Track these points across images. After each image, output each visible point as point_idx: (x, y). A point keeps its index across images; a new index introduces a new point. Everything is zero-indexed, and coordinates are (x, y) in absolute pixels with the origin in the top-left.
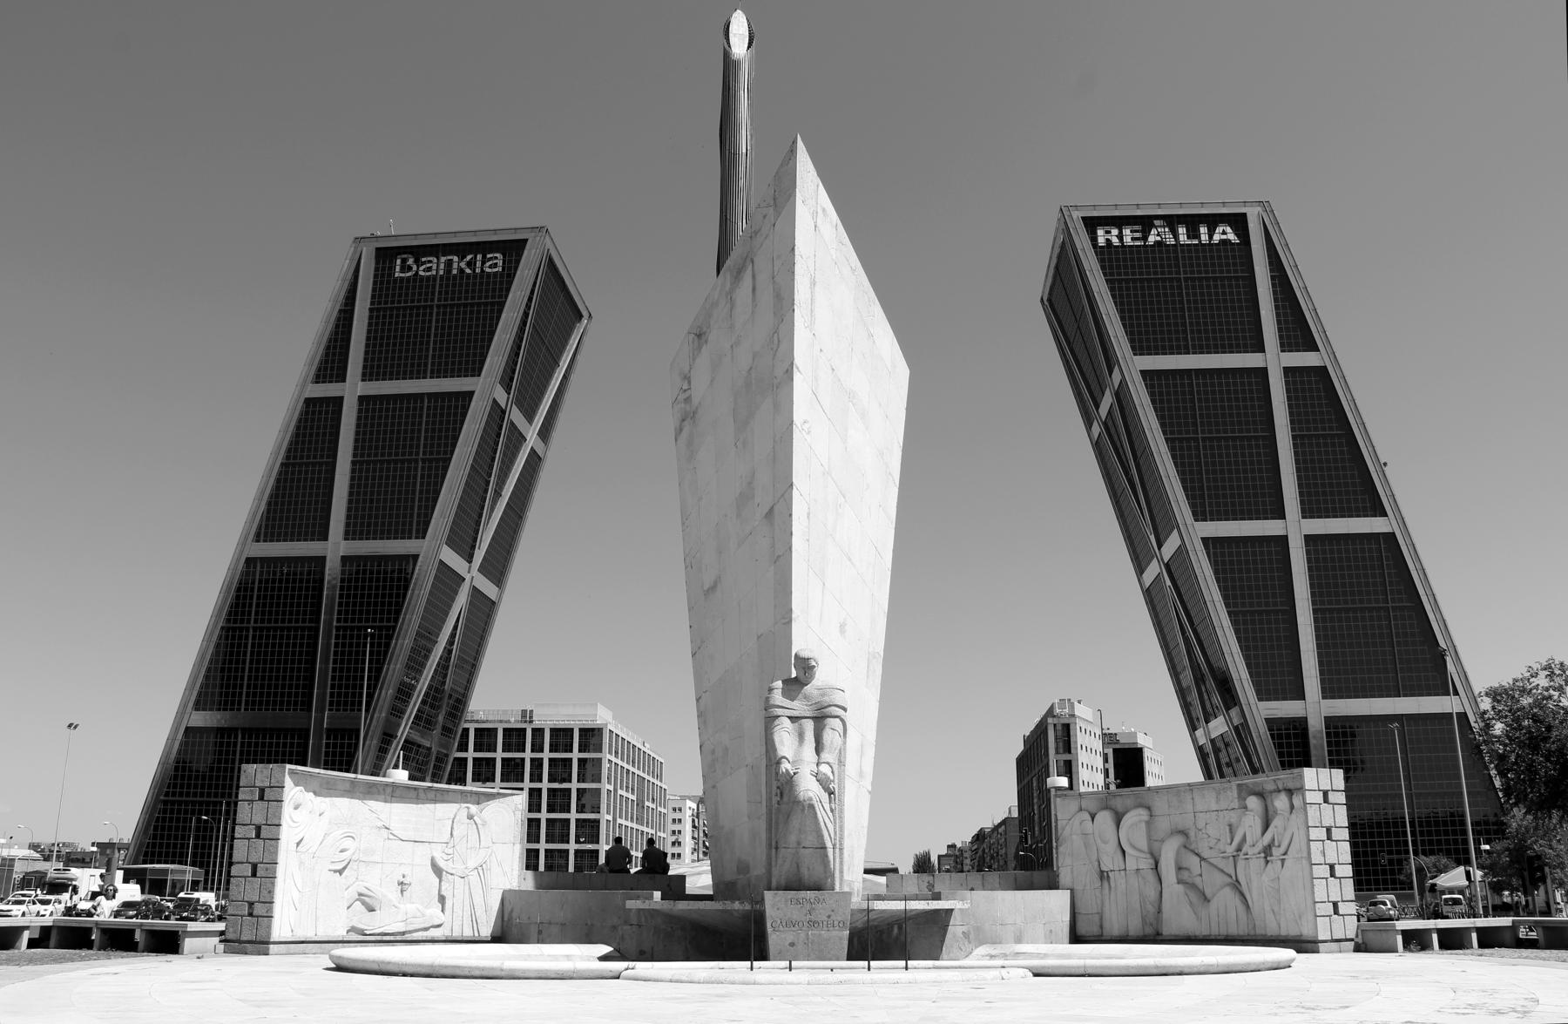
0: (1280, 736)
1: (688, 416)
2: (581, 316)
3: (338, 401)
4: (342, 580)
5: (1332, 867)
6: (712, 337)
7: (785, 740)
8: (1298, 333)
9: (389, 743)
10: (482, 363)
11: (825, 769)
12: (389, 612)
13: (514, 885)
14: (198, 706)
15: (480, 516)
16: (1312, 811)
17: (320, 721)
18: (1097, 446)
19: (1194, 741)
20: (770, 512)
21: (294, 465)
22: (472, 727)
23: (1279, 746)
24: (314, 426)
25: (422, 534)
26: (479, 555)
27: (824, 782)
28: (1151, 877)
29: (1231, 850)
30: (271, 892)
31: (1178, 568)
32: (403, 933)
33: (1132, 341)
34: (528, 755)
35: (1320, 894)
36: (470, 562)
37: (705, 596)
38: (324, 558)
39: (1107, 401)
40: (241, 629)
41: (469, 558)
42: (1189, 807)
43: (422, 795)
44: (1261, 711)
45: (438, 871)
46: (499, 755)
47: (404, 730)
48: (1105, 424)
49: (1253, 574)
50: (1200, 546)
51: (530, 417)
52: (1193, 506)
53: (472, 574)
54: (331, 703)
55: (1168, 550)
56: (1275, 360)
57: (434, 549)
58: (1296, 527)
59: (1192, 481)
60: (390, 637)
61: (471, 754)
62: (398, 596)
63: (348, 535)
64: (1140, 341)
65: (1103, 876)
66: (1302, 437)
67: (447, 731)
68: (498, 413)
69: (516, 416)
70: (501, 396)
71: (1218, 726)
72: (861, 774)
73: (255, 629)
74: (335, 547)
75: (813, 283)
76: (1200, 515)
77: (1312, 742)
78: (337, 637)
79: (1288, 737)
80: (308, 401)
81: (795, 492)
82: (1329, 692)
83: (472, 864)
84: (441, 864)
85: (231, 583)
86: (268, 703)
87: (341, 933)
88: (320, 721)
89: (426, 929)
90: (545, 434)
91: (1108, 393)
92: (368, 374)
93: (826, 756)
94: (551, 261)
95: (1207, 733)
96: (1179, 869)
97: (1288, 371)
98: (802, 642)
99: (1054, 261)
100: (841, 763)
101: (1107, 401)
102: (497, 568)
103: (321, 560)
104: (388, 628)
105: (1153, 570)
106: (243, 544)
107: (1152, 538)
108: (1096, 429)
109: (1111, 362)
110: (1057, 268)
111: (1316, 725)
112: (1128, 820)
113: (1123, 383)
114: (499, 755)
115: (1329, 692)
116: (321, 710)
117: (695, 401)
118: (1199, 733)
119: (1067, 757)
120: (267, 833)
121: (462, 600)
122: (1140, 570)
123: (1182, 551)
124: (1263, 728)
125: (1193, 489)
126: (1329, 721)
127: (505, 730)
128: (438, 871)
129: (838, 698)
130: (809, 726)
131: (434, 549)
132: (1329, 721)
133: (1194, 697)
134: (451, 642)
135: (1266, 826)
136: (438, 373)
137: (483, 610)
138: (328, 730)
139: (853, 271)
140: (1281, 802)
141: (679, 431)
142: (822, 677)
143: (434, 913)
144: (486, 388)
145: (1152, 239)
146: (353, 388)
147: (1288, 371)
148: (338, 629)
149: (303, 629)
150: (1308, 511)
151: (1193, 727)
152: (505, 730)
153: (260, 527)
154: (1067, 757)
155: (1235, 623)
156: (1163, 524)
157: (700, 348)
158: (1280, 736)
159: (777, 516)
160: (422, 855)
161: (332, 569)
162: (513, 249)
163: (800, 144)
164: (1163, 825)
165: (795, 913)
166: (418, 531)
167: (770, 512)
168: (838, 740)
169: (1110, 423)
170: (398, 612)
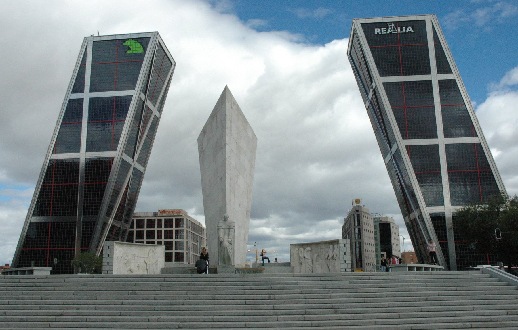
2: (172, 64)
3: (81, 101)
7: (221, 234)
8: (443, 67)
11: (230, 240)
14: (34, 215)
22: (135, 219)
26: (136, 156)
27: (230, 243)
30: (112, 268)
41: (133, 158)
44: (427, 211)
46: (146, 229)
47: (111, 221)
48: (371, 102)
55: (394, 149)
56: (435, 77)
58: (441, 141)
61: (135, 229)
62: (107, 172)
65: (301, 264)
69: (149, 104)
70: (143, 96)
72: (245, 239)
74: (83, 155)
76: (404, 137)
77: (447, 222)
80: (70, 100)
81: (227, 174)
83: (154, 262)
84: (147, 262)
91: (371, 90)
93: (231, 237)
94: (160, 44)
95: (409, 218)
100: (234, 238)
101: (371, 93)
104: (104, 184)
107: (388, 145)
108: (368, 104)
114: (146, 229)
119: (359, 227)
124: (428, 217)
129: (233, 224)
130: (227, 231)
135: (333, 252)
137: (139, 176)
145: (389, 32)
146: (87, 95)
169: (372, 102)
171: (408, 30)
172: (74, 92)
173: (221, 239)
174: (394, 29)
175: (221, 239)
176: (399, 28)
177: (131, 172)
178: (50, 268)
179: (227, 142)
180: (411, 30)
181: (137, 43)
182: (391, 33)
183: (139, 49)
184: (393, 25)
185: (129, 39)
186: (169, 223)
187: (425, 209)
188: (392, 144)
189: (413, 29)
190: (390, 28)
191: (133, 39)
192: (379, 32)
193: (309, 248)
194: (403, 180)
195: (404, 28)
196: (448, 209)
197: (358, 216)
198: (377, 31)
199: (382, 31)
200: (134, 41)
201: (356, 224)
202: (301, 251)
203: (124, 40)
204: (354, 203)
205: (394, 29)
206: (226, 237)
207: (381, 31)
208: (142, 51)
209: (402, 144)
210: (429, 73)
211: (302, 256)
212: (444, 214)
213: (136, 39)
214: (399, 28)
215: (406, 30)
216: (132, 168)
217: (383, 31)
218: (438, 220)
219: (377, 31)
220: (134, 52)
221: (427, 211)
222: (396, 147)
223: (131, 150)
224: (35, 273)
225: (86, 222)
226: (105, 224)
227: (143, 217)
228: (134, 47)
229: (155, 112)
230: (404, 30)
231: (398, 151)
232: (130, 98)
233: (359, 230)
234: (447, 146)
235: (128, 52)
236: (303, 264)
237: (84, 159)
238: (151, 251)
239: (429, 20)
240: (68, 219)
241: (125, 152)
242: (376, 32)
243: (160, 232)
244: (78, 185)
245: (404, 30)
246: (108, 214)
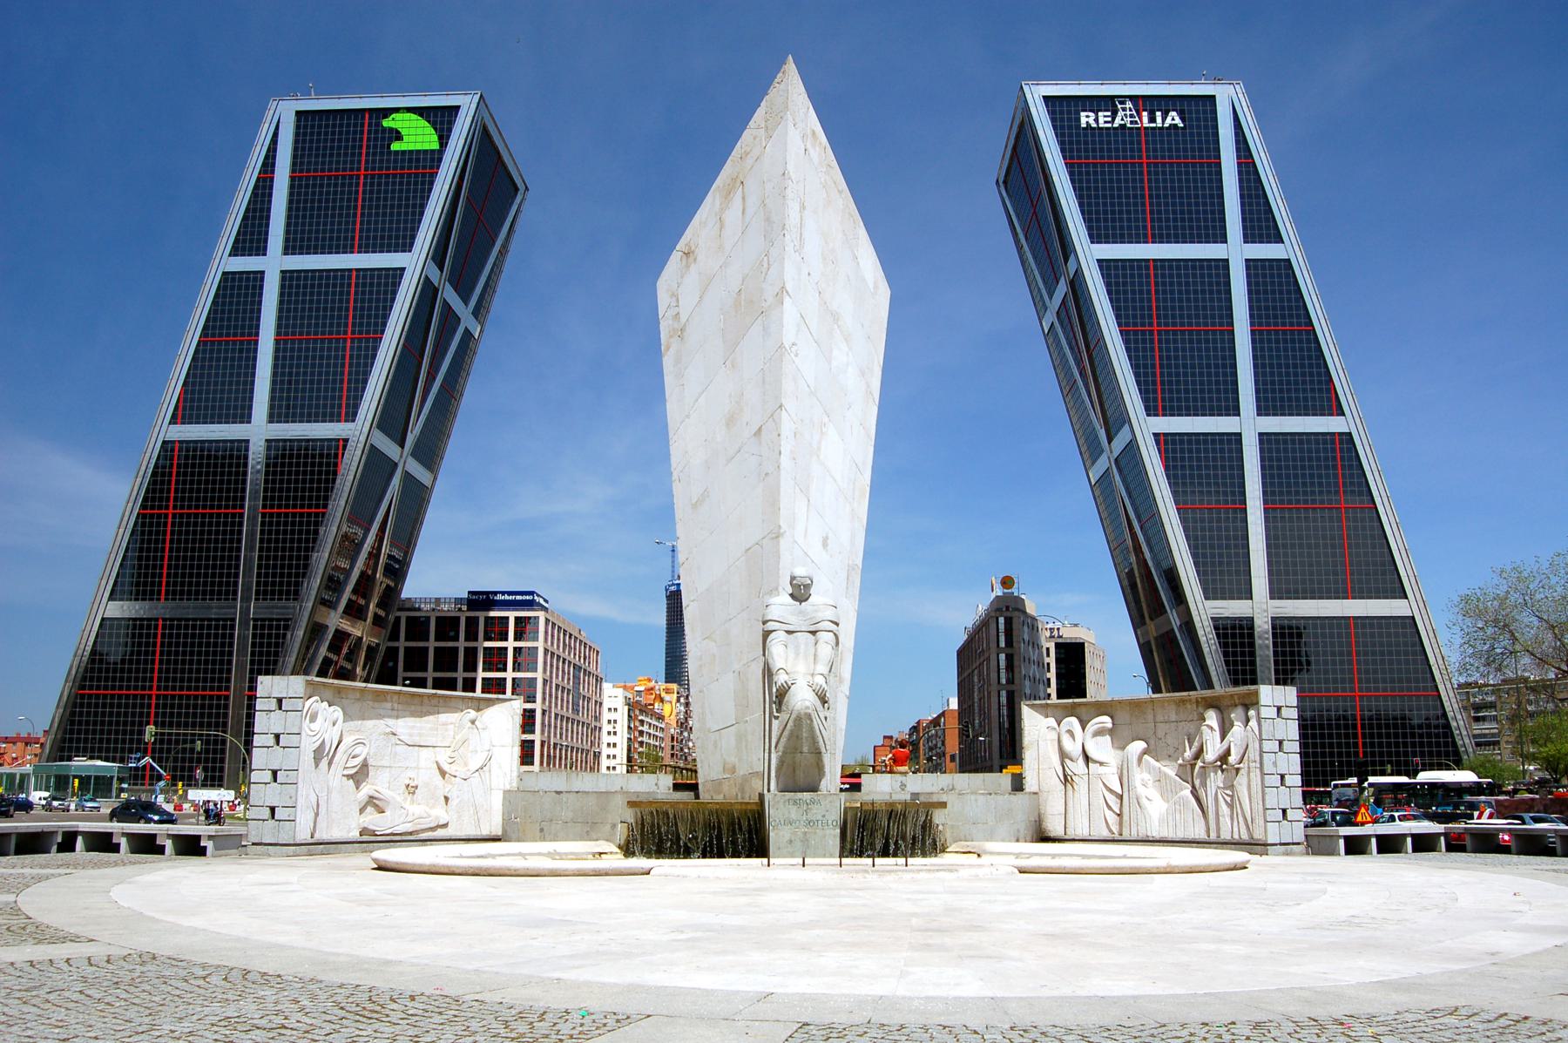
0: (1226, 636)
2: (517, 189)
4: (267, 465)
5: (1282, 777)
6: (701, 255)
8: (1260, 225)
10: (413, 237)
12: (318, 498)
16: (1265, 725)
23: (1224, 645)
25: (351, 416)
32: (411, 833)
33: (1089, 229)
34: (462, 644)
36: (402, 446)
41: (402, 446)
42: (1150, 717)
43: (426, 700)
46: (432, 644)
49: (1204, 468)
50: (1151, 441)
52: (1146, 401)
54: (258, 593)
56: (1236, 251)
58: (1249, 424)
59: (1146, 375)
63: (272, 418)
64: (1099, 228)
65: (1067, 780)
66: (1261, 332)
68: (428, 292)
69: (449, 294)
70: (435, 275)
74: (259, 431)
76: (1151, 410)
77: (1258, 642)
78: (263, 524)
82: (1276, 593)
84: (446, 767)
87: (354, 835)
89: (432, 829)
90: (476, 313)
92: (289, 249)
94: (485, 130)
97: (1250, 264)
101: (1062, 288)
102: (429, 453)
104: (317, 515)
105: (1103, 463)
108: (1050, 318)
109: (1067, 249)
111: (1262, 625)
113: (1079, 272)
114: (432, 644)
115: (1276, 593)
116: (246, 599)
117: (683, 319)
119: (1009, 651)
125: (1146, 383)
127: (438, 618)
137: (416, 499)
139: (840, 192)
143: (440, 814)
146: (274, 263)
148: (264, 516)
150: (1263, 409)
152: (438, 618)
154: (1009, 651)
156: (1115, 420)
157: (688, 266)
158: (1226, 636)
161: (257, 454)
165: (794, 813)
166: (347, 414)
170: (326, 498)
171: (1169, 121)
173: (781, 678)
175: (781, 678)
176: (1145, 114)
177: (396, 481)
180: (1178, 121)
181: (423, 123)
182: (1123, 127)
184: (1129, 105)
185: (397, 110)
188: (1113, 431)
189: (1183, 119)
190: (1121, 113)
192: (1091, 121)
193: (1106, 721)
195: (1158, 114)
198: (1086, 118)
199: (1101, 120)
200: (414, 116)
201: (1002, 644)
202: (1071, 733)
207: (1096, 120)
208: (436, 146)
209: (1146, 427)
210: (1223, 239)
211: (1073, 748)
214: (1145, 114)
215: (1164, 120)
218: (1236, 635)
219: (1086, 118)
220: (411, 147)
221: (1205, 610)
222: (1129, 437)
223: (392, 421)
225: (263, 620)
228: (412, 131)
229: (467, 320)
230: (1159, 119)
231: (1132, 448)
232: (394, 276)
233: (1009, 658)
234: (1264, 438)
235: (396, 146)
236: (1081, 785)
237: (263, 443)
239: (1228, 96)
240: (215, 609)
241: (379, 427)
242: (1083, 121)
245: (1159, 119)
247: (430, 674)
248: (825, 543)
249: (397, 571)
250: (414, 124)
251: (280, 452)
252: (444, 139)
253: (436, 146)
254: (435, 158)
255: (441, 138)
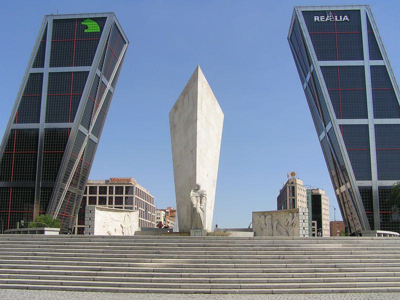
0: (363, 192)
1: (173, 126)
2: (126, 43)
4: (45, 137)
8: (376, 53)
9: (62, 192)
11: (202, 207)
13: (137, 230)
15: (92, 114)
16: (300, 217)
17: (38, 185)
18: (305, 90)
19: (336, 193)
20: (192, 150)
21: (27, 97)
22: (88, 186)
23: (362, 196)
24: (34, 81)
25: (72, 121)
27: (202, 209)
28: (271, 229)
29: (286, 224)
30: (94, 231)
31: (331, 135)
33: (317, 56)
34: (108, 195)
35: (301, 233)
37: (177, 168)
38: (38, 129)
39: (309, 76)
40: (10, 154)
44: (357, 184)
45: (122, 227)
46: (98, 195)
48: (308, 83)
50: (338, 128)
51: (108, 80)
53: (89, 134)
54: (42, 179)
56: (367, 63)
57: (75, 126)
58: (371, 121)
60: (62, 156)
67: (81, 188)
68: (98, 78)
69: (104, 79)
70: (99, 73)
71: (343, 188)
73: (15, 153)
74: (42, 125)
75: (202, 99)
76: (338, 117)
77: (374, 195)
79: (365, 192)
80: (31, 74)
83: (129, 226)
85: (6, 137)
86: (20, 179)
88: (38, 185)
90: (113, 85)
96: (277, 228)
97: (372, 67)
98: (198, 182)
99: (292, 26)
100: (205, 205)
101: (309, 76)
102: (97, 131)
103: (38, 130)
104: (61, 153)
105: (323, 135)
106: (9, 124)
108: (305, 85)
109: (310, 63)
110: (293, 29)
111: (375, 189)
112: (267, 217)
114: (98, 195)
118: (338, 190)
119: (293, 198)
120: (92, 219)
121: (85, 143)
122: (319, 135)
123: (332, 128)
124: (357, 189)
126: (379, 188)
128: (122, 227)
129: (205, 193)
131: (75, 126)
132: (379, 188)
133: (335, 179)
134: (82, 158)
136: (76, 65)
137: (93, 146)
138: (42, 188)
140: (295, 214)
141: (171, 130)
142: (202, 188)
144: (93, 70)
146: (47, 70)
147: (372, 67)
148: (44, 153)
149: (32, 153)
150: (376, 116)
151: (335, 188)
153: (16, 118)
154: (293, 198)
155: (349, 154)
158: (363, 192)
159: (193, 151)
160: (119, 224)
161: (41, 132)
162: (101, 21)
163: (200, 71)
164: (274, 218)
167: (192, 150)
168: (205, 201)
169: (310, 84)
170: (65, 148)
171: (344, 19)
172: (35, 66)
174: (332, 17)
178: (59, 229)
179: (198, 118)
180: (347, 19)
181: (94, 23)
183: (96, 28)
185: (86, 19)
186: (119, 190)
187: (354, 183)
190: (328, 16)
191: (90, 18)
192: (318, 19)
194: (336, 156)
195: (341, 16)
196: (375, 183)
197: (293, 188)
198: (316, 18)
201: (291, 195)
203: (83, 20)
204: (290, 175)
205: (332, 17)
206: (199, 204)
207: (320, 19)
208: (99, 31)
209: (337, 123)
212: (371, 187)
213: (94, 19)
216: (86, 139)
217: (322, 18)
218: (366, 193)
219: (316, 18)
220: (91, 31)
224: (46, 233)
226: (62, 190)
227: (96, 184)
228: (91, 26)
230: (341, 19)
231: (332, 128)
235: (86, 31)
238: (127, 216)
242: (315, 19)
243: (111, 198)
244: (37, 154)
245: (341, 19)
246: (65, 181)
247: (124, 206)
248: (207, 175)
249: (86, 171)
250: (92, 23)
251: (48, 131)
252: (102, 30)
253: (99, 31)
254: (99, 35)
255: (101, 28)
